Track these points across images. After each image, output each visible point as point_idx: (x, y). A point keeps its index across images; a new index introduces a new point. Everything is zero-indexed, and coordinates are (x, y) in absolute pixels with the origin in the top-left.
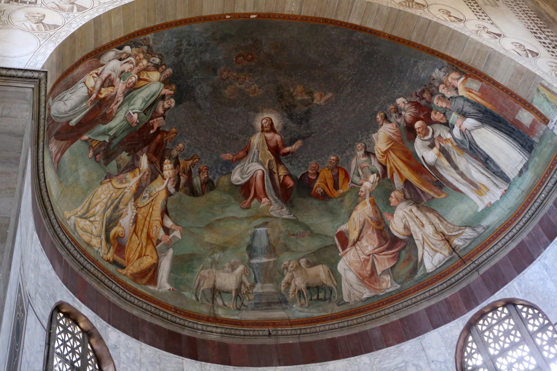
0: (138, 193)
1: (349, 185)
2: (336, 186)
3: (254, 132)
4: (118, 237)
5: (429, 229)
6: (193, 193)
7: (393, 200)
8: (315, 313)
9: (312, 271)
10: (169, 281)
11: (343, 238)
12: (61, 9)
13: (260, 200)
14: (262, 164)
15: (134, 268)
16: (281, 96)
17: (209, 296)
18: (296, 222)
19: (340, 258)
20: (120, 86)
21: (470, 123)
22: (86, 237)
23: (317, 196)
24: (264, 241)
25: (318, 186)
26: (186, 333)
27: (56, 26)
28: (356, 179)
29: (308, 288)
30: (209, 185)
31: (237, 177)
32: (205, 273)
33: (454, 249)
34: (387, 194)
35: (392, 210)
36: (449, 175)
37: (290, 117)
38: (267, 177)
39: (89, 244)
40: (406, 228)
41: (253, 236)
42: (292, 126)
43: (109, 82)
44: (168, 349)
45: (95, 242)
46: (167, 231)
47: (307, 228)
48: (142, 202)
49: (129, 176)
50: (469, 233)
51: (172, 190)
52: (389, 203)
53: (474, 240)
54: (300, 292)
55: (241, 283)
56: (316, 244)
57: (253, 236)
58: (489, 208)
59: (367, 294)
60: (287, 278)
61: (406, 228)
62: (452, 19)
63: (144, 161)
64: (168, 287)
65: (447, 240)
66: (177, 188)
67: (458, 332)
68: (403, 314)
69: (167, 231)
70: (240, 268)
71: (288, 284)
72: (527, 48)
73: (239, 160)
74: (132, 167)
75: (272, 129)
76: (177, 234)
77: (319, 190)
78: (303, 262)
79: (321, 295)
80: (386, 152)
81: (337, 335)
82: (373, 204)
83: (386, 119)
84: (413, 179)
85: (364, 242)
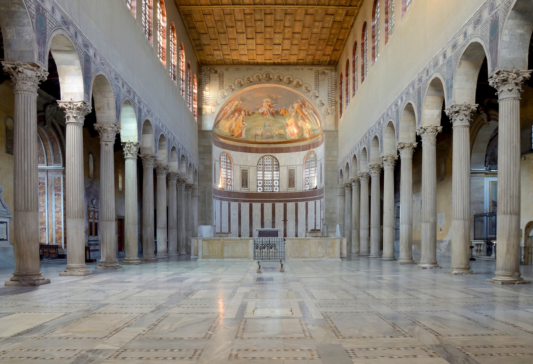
0: (235, 121)
1: (288, 114)
2: (285, 113)
3: (264, 102)
4: (232, 130)
6: (249, 115)
7: (299, 119)
9: (280, 131)
10: (245, 135)
11: (287, 125)
13: (266, 116)
14: (266, 108)
15: (236, 135)
16: (269, 96)
17: (255, 137)
18: (275, 120)
19: (286, 129)
20: (228, 109)
21: (312, 111)
22: (225, 134)
23: (280, 115)
24: (268, 124)
25: (281, 113)
27: (214, 112)
28: (290, 113)
30: (253, 113)
31: (260, 111)
32: (253, 131)
35: (299, 121)
37: (272, 100)
38: (268, 111)
39: (226, 135)
41: (265, 123)
42: (273, 101)
43: (226, 109)
44: (244, 152)
45: (227, 134)
47: (278, 122)
48: (236, 121)
49: (233, 118)
51: (244, 116)
52: (298, 119)
53: (313, 134)
55: (263, 133)
56: (281, 125)
57: (265, 123)
58: (316, 130)
60: (274, 131)
62: (307, 91)
63: (236, 114)
64: (245, 136)
66: (245, 116)
70: (262, 129)
71: (274, 133)
73: (260, 108)
74: (234, 116)
75: (268, 102)
77: (281, 114)
78: (277, 129)
79: (282, 136)
80: (297, 109)
82: (294, 118)
84: (303, 115)
85: (292, 126)
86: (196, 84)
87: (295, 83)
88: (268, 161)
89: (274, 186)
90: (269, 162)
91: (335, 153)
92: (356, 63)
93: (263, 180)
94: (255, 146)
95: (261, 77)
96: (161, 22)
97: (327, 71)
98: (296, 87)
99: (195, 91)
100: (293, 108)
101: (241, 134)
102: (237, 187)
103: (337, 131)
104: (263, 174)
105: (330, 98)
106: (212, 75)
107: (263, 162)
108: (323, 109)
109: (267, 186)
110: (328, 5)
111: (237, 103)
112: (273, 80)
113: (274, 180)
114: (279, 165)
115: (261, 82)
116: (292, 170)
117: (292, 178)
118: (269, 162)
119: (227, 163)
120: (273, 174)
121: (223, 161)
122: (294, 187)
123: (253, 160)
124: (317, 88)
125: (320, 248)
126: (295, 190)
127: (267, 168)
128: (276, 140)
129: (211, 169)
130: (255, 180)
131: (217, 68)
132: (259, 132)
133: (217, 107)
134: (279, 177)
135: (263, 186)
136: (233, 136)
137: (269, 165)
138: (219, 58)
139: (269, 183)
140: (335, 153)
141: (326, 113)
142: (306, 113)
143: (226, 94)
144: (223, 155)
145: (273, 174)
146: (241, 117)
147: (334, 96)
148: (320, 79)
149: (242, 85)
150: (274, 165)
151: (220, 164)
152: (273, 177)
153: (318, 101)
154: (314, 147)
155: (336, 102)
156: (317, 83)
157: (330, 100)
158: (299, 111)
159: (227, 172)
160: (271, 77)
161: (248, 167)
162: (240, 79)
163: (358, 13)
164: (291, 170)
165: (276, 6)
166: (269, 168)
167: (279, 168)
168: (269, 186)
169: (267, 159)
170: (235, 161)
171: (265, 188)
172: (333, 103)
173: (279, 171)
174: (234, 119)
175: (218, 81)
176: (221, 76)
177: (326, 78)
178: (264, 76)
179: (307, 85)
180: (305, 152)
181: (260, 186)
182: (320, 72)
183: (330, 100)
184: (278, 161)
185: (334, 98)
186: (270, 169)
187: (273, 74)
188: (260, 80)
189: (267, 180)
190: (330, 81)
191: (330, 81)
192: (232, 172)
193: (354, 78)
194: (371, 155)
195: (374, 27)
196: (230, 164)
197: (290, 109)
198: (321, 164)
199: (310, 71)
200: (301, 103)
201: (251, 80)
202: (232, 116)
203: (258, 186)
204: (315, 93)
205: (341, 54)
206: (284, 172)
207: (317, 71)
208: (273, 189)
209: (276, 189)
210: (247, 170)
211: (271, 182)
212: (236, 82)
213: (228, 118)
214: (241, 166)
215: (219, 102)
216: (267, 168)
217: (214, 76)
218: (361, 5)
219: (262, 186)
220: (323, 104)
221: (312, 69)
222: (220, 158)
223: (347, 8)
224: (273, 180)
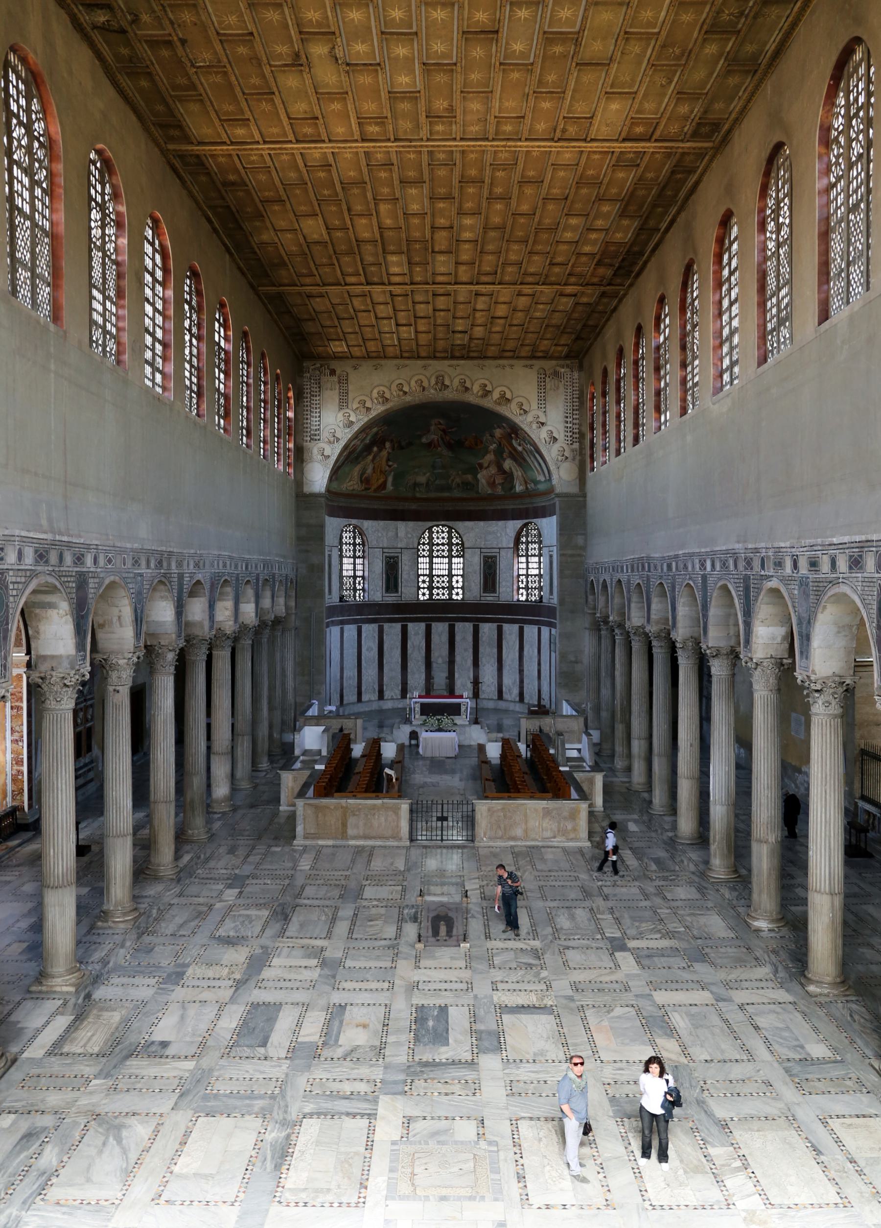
0: (373, 460)
2: (476, 445)
5: (520, 474)
6: (401, 448)
7: (505, 456)
8: (464, 495)
10: (393, 485)
12: (330, 442)
15: (373, 488)
22: (351, 488)
26: (401, 508)
27: (329, 456)
29: (463, 483)
33: (527, 488)
34: (502, 453)
35: (504, 460)
36: (528, 459)
40: (510, 468)
45: (356, 487)
46: (390, 466)
50: (532, 485)
51: (390, 451)
53: (534, 490)
54: (458, 485)
58: (540, 482)
59: (490, 492)
61: (510, 468)
62: (522, 411)
63: (375, 449)
65: (526, 483)
66: (393, 449)
67: (519, 526)
68: (503, 507)
69: (390, 466)
71: (453, 481)
72: (554, 435)
74: (369, 454)
76: (395, 466)
81: (472, 508)
82: (495, 455)
83: (499, 427)
86: (292, 401)
87: (496, 395)
88: (440, 534)
89: (453, 588)
90: (443, 538)
91: (580, 540)
92: (622, 384)
93: (431, 576)
94: (413, 506)
95: (425, 384)
96: (222, 344)
97: (563, 370)
98: (499, 404)
99: (291, 414)
100: (491, 436)
101: (383, 486)
102: (378, 595)
103: (584, 496)
104: (431, 563)
105: (569, 425)
106: (324, 379)
107: (431, 538)
108: (556, 447)
109: (438, 588)
110: (565, 284)
111: (375, 430)
112: (450, 390)
113: (453, 576)
114: (463, 544)
115: (426, 393)
116: (491, 557)
117: (490, 574)
118: (443, 538)
119: (354, 544)
120: (450, 563)
121: (346, 544)
122: (494, 591)
123: (410, 536)
124: (543, 406)
125: (547, 820)
126: (496, 599)
127: (438, 551)
128: (457, 494)
129: (323, 571)
130: (413, 577)
131: (334, 364)
132: (422, 479)
133: (336, 444)
134: (463, 569)
135: (431, 588)
136: (366, 489)
137: (443, 544)
138: (339, 349)
139: (443, 582)
140: (580, 540)
141: (560, 458)
142: (520, 448)
143: (353, 418)
144: (346, 531)
145: (450, 563)
146: (384, 453)
147: (577, 421)
148: (548, 387)
149: (387, 400)
150: (453, 544)
151: (341, 550)
152: (450, 569)
153: (543, 434)
154: (536, 516)
155: (582, 435)
156: (543, 395)
157: (569, 430)
158: (504, 442)
159: (354, 564)
160: (447, 382)
161: (400, 550)
162: (382, 388)
163: (624, 295)
164: (489, 557)
165: (456, 286)
166: (443, 551)
167: (463, 551)
168: (443, 588)
169: (438, 532)
170: (372, 538)
171: (435, 591)
172: (574, 436)
173: (463, 556)
174: (370, 457)
175: (337, 391)
176: (343, 381)
177: (561, 385)
178: (433, 381)
179: (521, 400)
180: (519, 524)
181: (424, 588)
182: (548, 373)
183: (569, 430)
184: (460, 537)
185: (577, 426)
186: (446, 554)
187: (450, 377)
188: (424, 389)
189: (438, 576)
190: (569, 391)
191: (569, 391)
192: (366, 562)
193: (618, 416)
194: (653, 612)
195: (658, 348)
196: (364, 546)
197: (487, 437)
198: (551, 556)
199: (528, 370)
200: (509, 430)
201: (406, 389)
202: (365, 453)
203: (419, 588)
204: (538, 417)
205: (591, 345)
206: (476, 560)
207: (541, 371)
208: (450, 594)
209: (457, 594)
210: (397, 557)
211: (446, 579)
212: (375, 394)
213: (357, 458)
214: (385, 550)
215: (338, 435)
216: (438, 551)
217: (329, 381)
218: (631, 285)
219: (428, 588)
220: (555, 439)
221: (531, 366)
222: (341, 538)
223: (602, 288)
224: (450, 576)
